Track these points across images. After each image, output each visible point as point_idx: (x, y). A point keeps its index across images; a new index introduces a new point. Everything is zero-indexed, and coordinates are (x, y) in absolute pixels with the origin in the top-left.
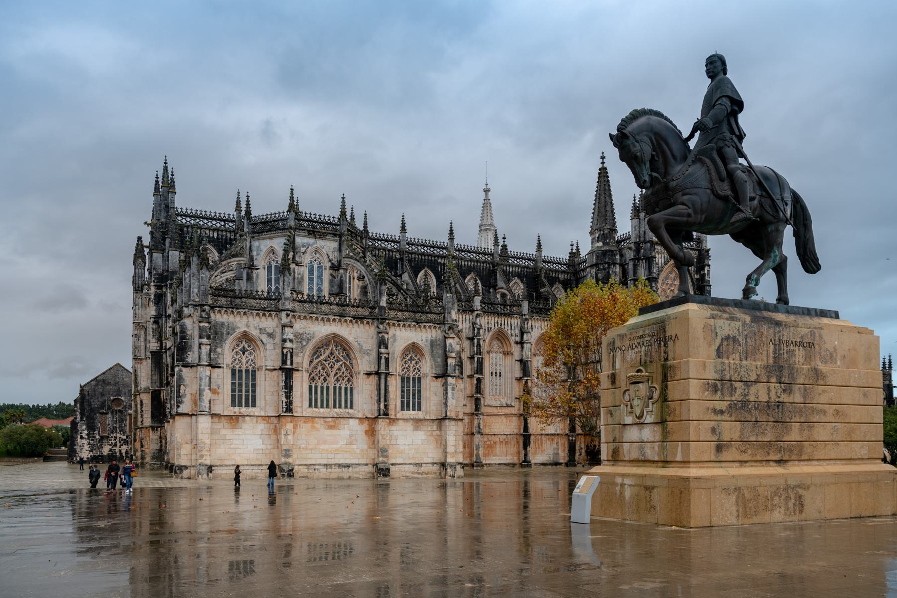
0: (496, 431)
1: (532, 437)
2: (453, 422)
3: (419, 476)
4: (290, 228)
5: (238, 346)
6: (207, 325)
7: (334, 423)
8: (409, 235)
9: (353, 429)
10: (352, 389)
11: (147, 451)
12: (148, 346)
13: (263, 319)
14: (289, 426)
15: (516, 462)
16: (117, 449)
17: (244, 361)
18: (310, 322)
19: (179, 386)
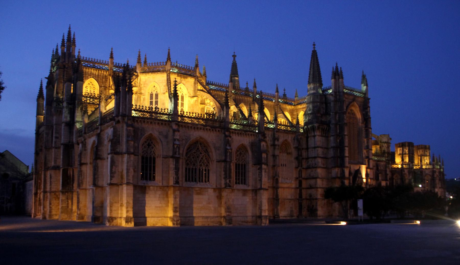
1: (280, 201)
6: (131, 129)
10: (208, 170)
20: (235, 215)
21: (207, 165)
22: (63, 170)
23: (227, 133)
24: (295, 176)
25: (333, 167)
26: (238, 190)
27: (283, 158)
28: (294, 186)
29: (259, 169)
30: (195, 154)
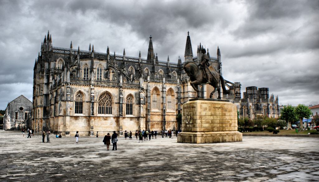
1: (166, 122)
2: (142, 118)
5: (77, 95)
6: (69, 89)
7: (106, 119)
8: (126, 55)
10: (111, 108)
11: (40, 126)
12: (41, 91)
13: (85, 86)
14: (93, 119)
16: (21, 125)
17: (79, 99)
18: (99, 87)
19: (60, 107)
21: (110, 105)
24: (176, 108)
26: (128, 117)
27: (169, 98)
28: (175, 114)
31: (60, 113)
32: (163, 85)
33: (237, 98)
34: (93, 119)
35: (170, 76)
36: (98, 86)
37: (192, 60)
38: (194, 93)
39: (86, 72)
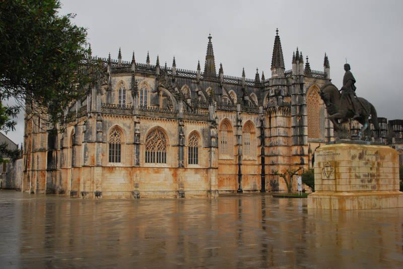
0: (224, 172)
1: (243, 176)
2: (214, 170)
3: (198, 197)
4: (133, 72)
6: (100, 122)
7: (157, 171)
8: (179, 67)
9: (168, 173)
10: (165, 153)
13: (125, 119)
14: (138, 172)
15: (235, 189)
17: (115, 140)
20: (188, 189)
21: (164, 149)
22: (48, 152)
23: (181, 123)
25: (293, 146)
27: (247, 137)
29: (209, 151)
30: (154, 140)
31: (85, 162)
32: (237, 116)
33: (353, 137)
34: (138, 172)
35: (245, 102)
36: (145, 118)
37: (283, 76)
38: (287, 129)
39: (122, 95)
